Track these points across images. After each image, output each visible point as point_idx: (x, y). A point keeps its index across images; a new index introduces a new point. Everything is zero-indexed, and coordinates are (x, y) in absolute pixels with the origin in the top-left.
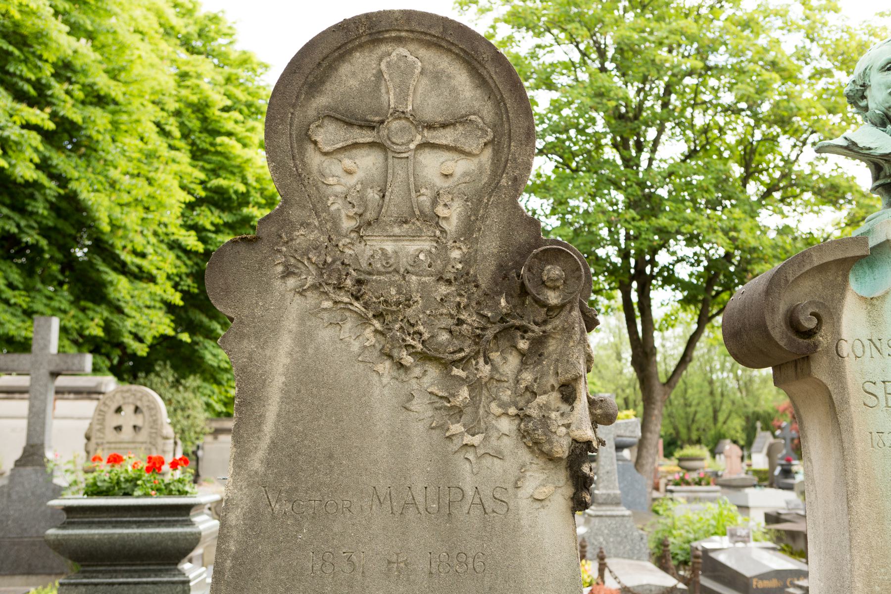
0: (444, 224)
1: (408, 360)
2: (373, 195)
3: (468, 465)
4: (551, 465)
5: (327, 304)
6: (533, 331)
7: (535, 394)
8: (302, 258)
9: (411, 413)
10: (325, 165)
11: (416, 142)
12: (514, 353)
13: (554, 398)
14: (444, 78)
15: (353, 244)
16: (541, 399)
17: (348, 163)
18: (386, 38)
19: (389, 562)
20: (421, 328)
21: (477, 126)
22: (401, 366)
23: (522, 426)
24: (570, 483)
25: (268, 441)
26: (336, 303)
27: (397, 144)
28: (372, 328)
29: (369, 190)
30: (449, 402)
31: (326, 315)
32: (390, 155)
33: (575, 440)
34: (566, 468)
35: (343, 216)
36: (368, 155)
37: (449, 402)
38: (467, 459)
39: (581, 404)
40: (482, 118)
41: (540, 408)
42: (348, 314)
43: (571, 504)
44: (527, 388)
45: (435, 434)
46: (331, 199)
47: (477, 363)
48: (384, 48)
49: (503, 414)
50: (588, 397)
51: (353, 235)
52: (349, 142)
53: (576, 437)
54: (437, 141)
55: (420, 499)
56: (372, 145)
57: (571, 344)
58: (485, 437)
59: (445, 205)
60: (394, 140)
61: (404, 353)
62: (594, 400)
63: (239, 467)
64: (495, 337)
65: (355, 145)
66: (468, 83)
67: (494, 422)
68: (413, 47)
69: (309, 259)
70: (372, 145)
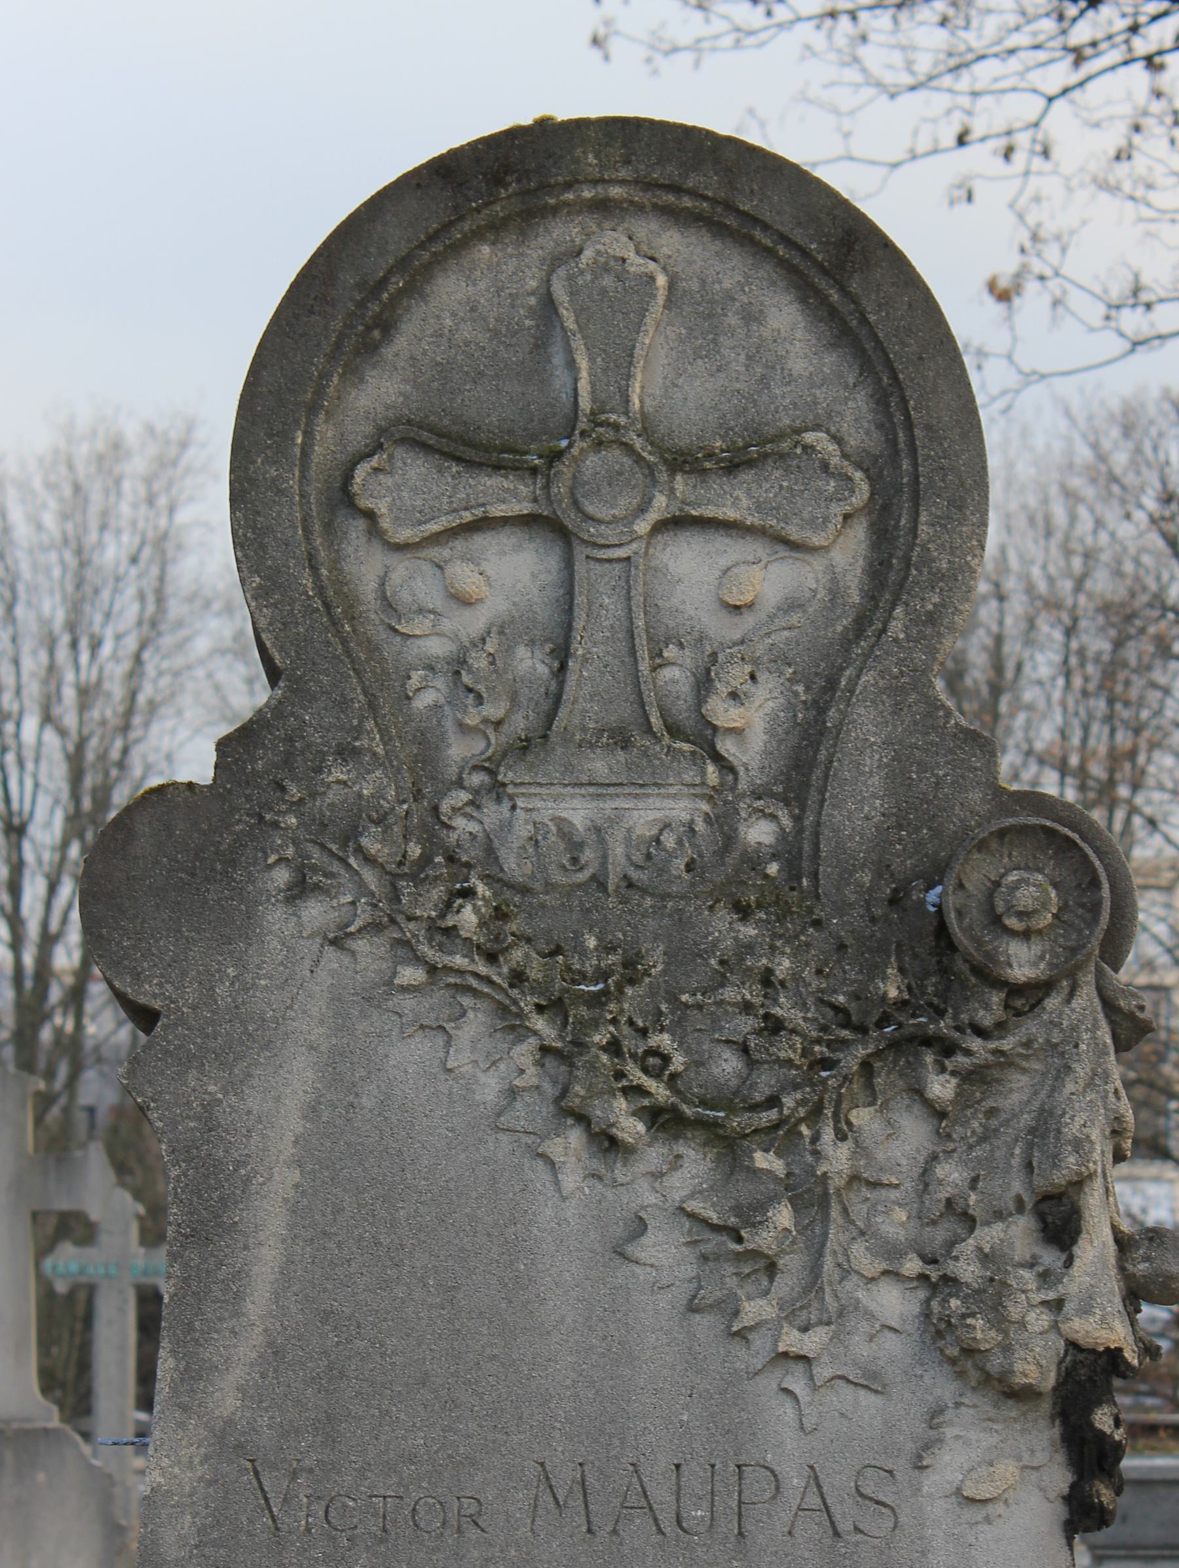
0: (727, 746)
1: (631, 1128)
5: (411, 975)
6: (968, 1053)
7: (970, 1222)
8: (344, 846)
9: (638, 1270)
10: (396, 577)
11: (653, 516)
12: (917, 1109)
14: (733, 320)
16: (989, 1235)
17: (465, 576)
18: (567, 204)
20: (664, 1041)
21: (825, 466)
23: (935, 1304)
24: (1060, 1457)
26: (432, 970)
27: (600, 522)
28: (533, 1041)
29: (522, 652)
30: (739, 1240)
31: (408, 1003)
32: (580, 552)
33: (1072, 1345)
35: (449, 724)
36: (517, 548)
37: (739, 1240)
38: (786, 1391)
40: (837, 439)
41: (985, 1258)
42: (467, 1001)
44: (949, 1202)
45: (705, 1324)
46: (416, 677)
47: (815, 1139)
49: (885, 1273)
50: (1114, 1228)
51: (477, 779)
52: (467, 516)
54: (709, 512)
55: (662, 1495)
57: (1070, 1087)
59: (734, 695)
60: (590, 509)
61: (621, 1103)
62: (1131, 1237)
63: (185, 1408)
64: (866, 1067)
66: (799, 334)
68: (645, 227)
69: (359, 850)
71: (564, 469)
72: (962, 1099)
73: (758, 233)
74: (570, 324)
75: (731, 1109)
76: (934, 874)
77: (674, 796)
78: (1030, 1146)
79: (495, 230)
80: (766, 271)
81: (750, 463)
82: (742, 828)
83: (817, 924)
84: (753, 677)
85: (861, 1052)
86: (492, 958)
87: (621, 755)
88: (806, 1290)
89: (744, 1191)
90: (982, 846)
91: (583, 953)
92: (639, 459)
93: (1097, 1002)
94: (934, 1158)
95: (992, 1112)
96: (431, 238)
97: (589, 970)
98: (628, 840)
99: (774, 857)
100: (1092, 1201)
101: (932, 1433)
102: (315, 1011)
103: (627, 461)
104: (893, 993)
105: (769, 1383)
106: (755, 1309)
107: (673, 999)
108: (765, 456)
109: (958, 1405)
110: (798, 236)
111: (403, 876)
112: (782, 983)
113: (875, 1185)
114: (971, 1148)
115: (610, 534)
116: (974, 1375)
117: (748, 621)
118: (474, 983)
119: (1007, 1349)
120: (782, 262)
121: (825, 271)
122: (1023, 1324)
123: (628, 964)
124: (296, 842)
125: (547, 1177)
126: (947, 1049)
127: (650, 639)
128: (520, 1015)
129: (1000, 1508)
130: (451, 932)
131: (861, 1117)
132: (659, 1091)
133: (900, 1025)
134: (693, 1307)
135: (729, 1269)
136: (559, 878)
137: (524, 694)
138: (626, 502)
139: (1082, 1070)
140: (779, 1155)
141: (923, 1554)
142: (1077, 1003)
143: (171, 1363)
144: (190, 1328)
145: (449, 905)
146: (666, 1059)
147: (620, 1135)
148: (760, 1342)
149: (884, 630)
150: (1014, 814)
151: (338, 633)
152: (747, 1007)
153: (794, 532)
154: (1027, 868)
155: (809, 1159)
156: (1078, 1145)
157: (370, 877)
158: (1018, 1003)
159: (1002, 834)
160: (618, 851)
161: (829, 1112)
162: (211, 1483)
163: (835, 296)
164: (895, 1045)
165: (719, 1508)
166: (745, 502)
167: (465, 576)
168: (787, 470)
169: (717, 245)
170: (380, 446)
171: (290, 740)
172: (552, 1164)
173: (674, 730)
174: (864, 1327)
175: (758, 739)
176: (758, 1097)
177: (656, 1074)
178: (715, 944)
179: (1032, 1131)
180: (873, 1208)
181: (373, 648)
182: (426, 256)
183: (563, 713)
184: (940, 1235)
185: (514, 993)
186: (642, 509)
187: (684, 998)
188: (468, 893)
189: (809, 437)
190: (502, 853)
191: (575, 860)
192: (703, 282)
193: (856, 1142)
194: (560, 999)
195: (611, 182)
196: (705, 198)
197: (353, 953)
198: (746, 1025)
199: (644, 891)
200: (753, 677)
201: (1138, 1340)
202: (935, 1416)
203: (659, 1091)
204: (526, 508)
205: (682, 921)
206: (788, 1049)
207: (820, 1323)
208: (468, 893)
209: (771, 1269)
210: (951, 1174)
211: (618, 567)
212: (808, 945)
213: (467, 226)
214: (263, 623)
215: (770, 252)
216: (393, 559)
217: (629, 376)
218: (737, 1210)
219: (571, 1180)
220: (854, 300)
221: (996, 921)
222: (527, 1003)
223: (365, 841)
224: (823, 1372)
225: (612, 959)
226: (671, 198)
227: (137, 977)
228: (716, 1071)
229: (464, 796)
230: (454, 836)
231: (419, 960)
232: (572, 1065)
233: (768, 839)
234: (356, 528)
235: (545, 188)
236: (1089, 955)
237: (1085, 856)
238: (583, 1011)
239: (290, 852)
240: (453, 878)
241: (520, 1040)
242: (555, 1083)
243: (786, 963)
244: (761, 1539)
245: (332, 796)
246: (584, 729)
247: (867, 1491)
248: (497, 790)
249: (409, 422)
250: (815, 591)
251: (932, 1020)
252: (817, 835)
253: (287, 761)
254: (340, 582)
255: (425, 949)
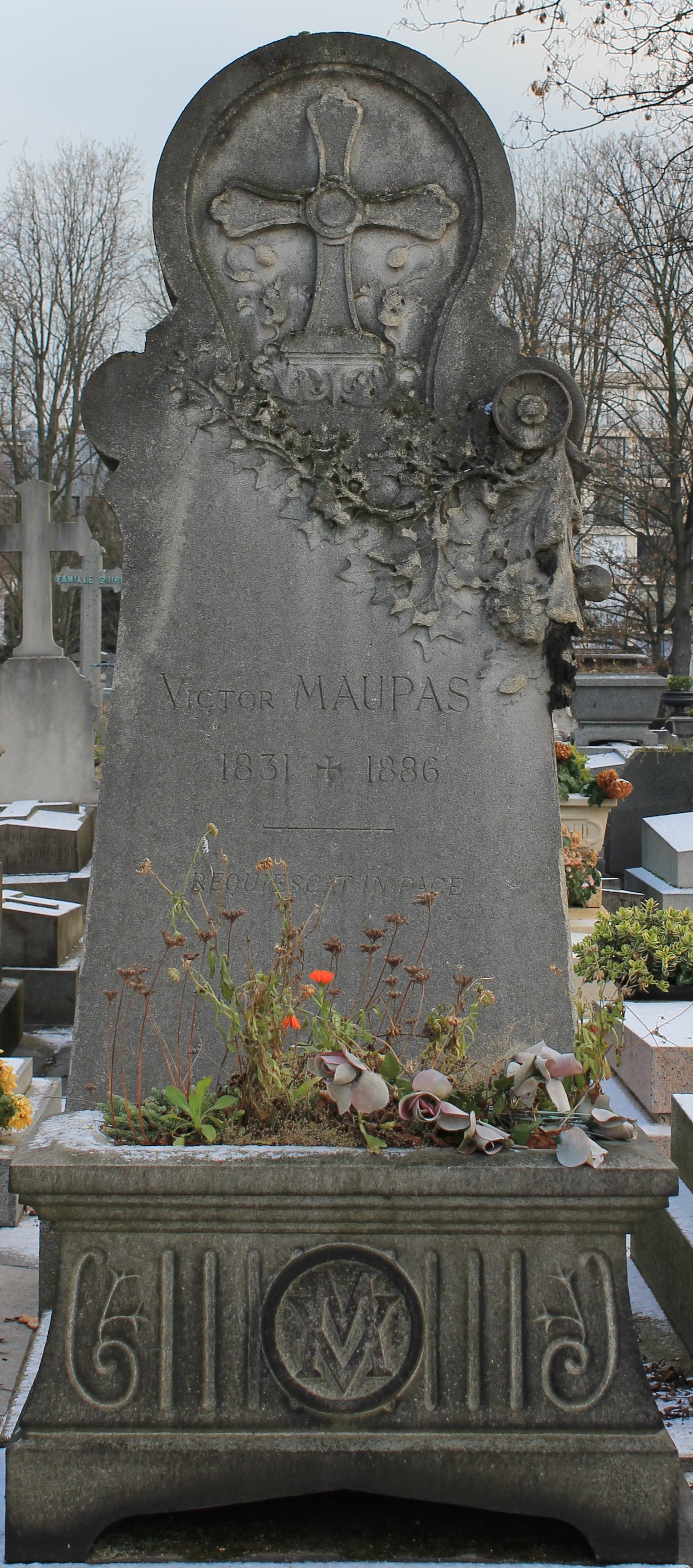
0: (390, 335)
1: (344, 517)
2: (296, 295)
3: (418, 652)
4: (523, 651)
5: (239, 444)
6: (504, 482)
7: (505, 563)
8: (207, 382)
9: (347, 585)
10: (231, 254)
11: (355, 224)
12: (480, 509)
13: (527, 569)
14: (394, 130)
15: (271, 364)
16: (514, 569)
17: (265, 253)
18: (314, 73)
19: (319, 767)
20: (360, 476)
21: (438, 201)
22: (332, 524)
23: (487, 601)
24: (546, 674)
25: (165, 615)
26: (249, 441)
27: (330, 227)
28: (297, 476)
29: (292, 289)
30: (395, 570)
31: (237, 457)
32: (320, 241)
33: (552, 621)
34: (543, 655)
35: (257, 324)
36: (290, 240)
37: (395, 570)
38: (417, 642)
39: (564, 575)
40: (444, 187)
41: (511, 579)
42: (265, 456)
43: (546, 699)
44: (495, 553)
45: (377, 610)
46: (242, 301)
47: (431, 522)
48: (312, 87)
49: (464, 586)
50: (573, 565)
51: (271, 350)
52: (266, 224)
53: (556, 617)
54: (382, 222)
55: (358, 691)
56: (295, 227)
57: (552, 498)
58: (440, 616)
59: (393, 311)
60: (325, 221)
61: (339, 506)
62: (581, 570)
63: (131, 649)
64: (456, 488)
65: (273, 228)
66: (426, 137)
67: (452, 597)
68: (353, 85)
69: (214, 384)
70: (295, 227)
71: (313, 201)
72: (501, 504)
73: (406, 88)
74: (316, 132)
75: (391, 508)
76: (489, 396)
77: (365, 359)
78: (533, 526)
79: (280, 86)
80: (410, 106)
81: (402, 199)
82: (397, 375)
83: (433, 420)
84: (403, 302)
85: (453, 481)
86: (277, 436)
87: (339, 339)
88: (426, 595)
89: (397, 547)
90: (511, 383)
91: (321, 433)
92: (349, 197)
93: (566, 458)
94: (487, 532)
95: (515, 510)
96: (250, 90)
97: (324, 442)
98: (342, 380)
99: (413, 388)
100: (563, 553)
101: (486, 662)
102: (193, 461)
103: (343, 198)
104: (469, 453)
105: (408, 638)
106: (402, 604)
107: (364, 455)
108: (409, 196)
109: (498, 649)
110: (426, 89)
111: (235, 397)
112: (416, 448)
113: (460, 545)
114: (505, 527)
115: (334, 233)
116: (506, 635)
117: (401, 274)
118: (269, 448)
119: (521, 622)
120: (418, 102)
121: (439, 107)
122: (529, 611)
123: (343, 439)
124: (184, 380)
125: (304, 540)
126: (494, 480)
127: (353, 283)
128: (291, 463)
129: (518, 697)
130: (258, 423)
131: (453, 512)
132: (357, 500)
133: (472, 469)
134: (372, 602)
135: (390, 584)
136: (309, 398)
137: (293, 310)
138: (342, 218)
139: (558, 490)
140: (414, 530)
141: (481, 719)
142: (557, 458)
143: (125, 628)
144: (134, 611)
145: (257, 410)
146: (360, 485)
147: (338, 520)
148: (405, 619)
149: (466, 280)
150: (527, 368)
151: (205, 280)
152: (399, 460)
153: (423, 232)
154: (533, 394)
155: (428, 532)
156: (556, 526)
157: (219, 397)
158: (529, 458)
159: (521, 377)
160: (338, 385)
161: (437, 510)
162: (144, 684)
163: (443, 119)
164: (471, 478)
165: (385, 697)
166: (399, 218)
167: (265, 253)
168: (420, 203)
169: (387, 94)
170: (224, 191)
171: (181, 331)
172: (306, 534)
173: (365, 327)
174: (454, 612)
175: (405, 331)
176: (404, 503)
177: (356, 492)
178: (384, 430)
179: (534, 519)
180: (458, 557)
181: (221, 288)
182: (247, 98)
183: (311, 319)
184: (490, 568)
185: (288, 452)
186: (350, 221)
187: (369, 455)
188: (266, 405)
189: (431, 187)
190: (282, 386)
191: (317, 389)
192: (380, 111)
193: (451, 524)
194: (310, 456)
195: (335, 63)
196: (381, 71)
197: (211, 434)
198: (399, 468)
199: (350, 404)
200: (403, 302)
201: (584, 618)
202: (487, 654)
203: (357, 500)
204: (294, 220)
205: (368, 419)
206: (419, 480)
207: (433, 610)
208: (266, 405)
209: (410, 584)
210: (496, 540)
211: (338, 248)
212: (428, 430)
213: (266, 84)
214: (168, 276)
215: (412, 97)
216: (231, 244)
217: (344, 157)
218: (394, 556)
219: (315, 542)
220: (452, 120)
221: (518, 419)
222: (294, 457)
223: (217, 380)
224: (434, 633)
225: (335, 436)
226: (365, 71)
227: (108, 444)
228: (384, 490)
229: (264, 358)
230: (259, 378)
231: (243, 437)
232: (315, 487)
233: (410, 380)
234: (213, 230)
235: (304, 66)
236: (562, 435)
237: (561, 389)
238: (321, 461)
239: (181, 385)
240: (259, 397)
241: (291, 475)
242: (307, 496)
243: (418, 439)
244: (404, 712)
245: (201, 358)
246: (322, 326)
247: (455, 689)
248: (280, 356)
249: (239, 178)
250: (433, 261)
251: (487, 466)
252: (433, 377)
253: (180, 342)
254: (205, 256)
255: (245, 432)
